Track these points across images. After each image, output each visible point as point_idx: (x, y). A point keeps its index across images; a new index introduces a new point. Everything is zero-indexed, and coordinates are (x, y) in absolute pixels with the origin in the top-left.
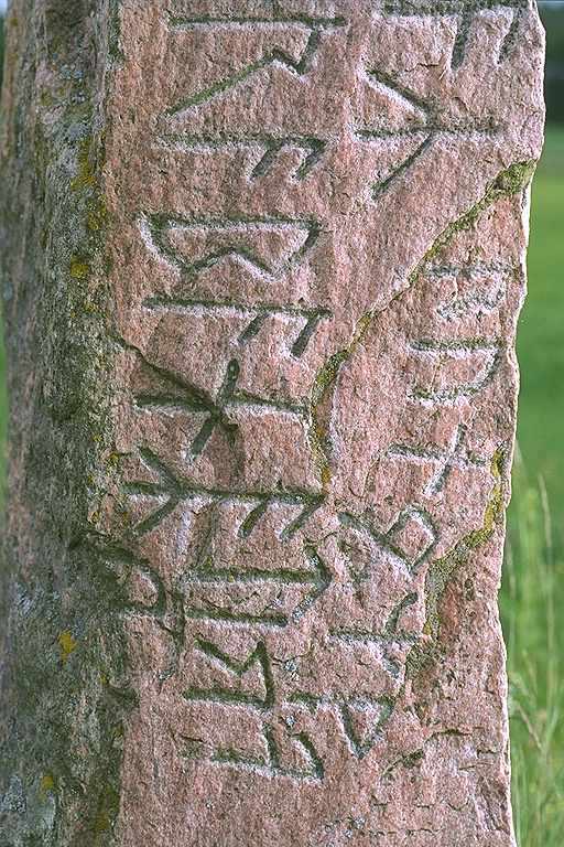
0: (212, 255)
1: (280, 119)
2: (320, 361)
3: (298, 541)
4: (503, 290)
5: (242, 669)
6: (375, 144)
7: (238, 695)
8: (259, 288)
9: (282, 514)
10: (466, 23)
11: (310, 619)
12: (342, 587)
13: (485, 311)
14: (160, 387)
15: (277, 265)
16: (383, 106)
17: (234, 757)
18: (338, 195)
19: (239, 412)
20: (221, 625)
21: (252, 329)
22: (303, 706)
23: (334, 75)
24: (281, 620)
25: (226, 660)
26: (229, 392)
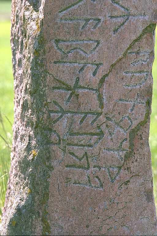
0: (72, 50)
1: (89, 13)
2: (100, 78)
3: (95, 124)
4: (148, 57)
5: (80, 160)
6: (114, 19)
7: (79, 167)
9: (90, 118)
11: (98, 146)
13: (143, 63)
15: (88, 52)
16: (115, 9)
17: (79, 183)
20: (76, 148)
21: (82, 69)
22: (97, 169)
24: (90, 146)
25: (76, 157)
26: (77, 86)
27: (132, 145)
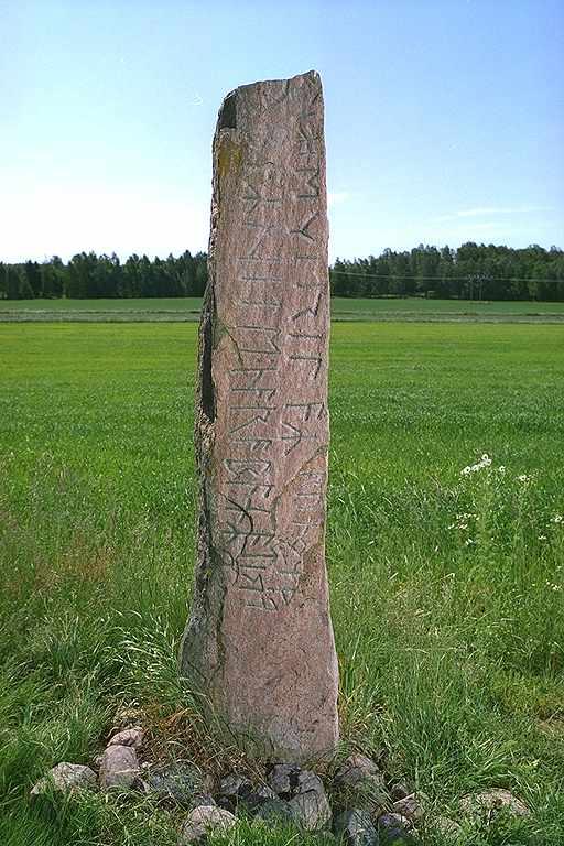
3: (268, 547)
8: (255, 479)
10: (309, 408)
12: (281, 558)
14: (233, 506)
16: (287, 431)
18: (276, 453)
19: (251, 512)
23: (274, 423)
27: (306, 567)
